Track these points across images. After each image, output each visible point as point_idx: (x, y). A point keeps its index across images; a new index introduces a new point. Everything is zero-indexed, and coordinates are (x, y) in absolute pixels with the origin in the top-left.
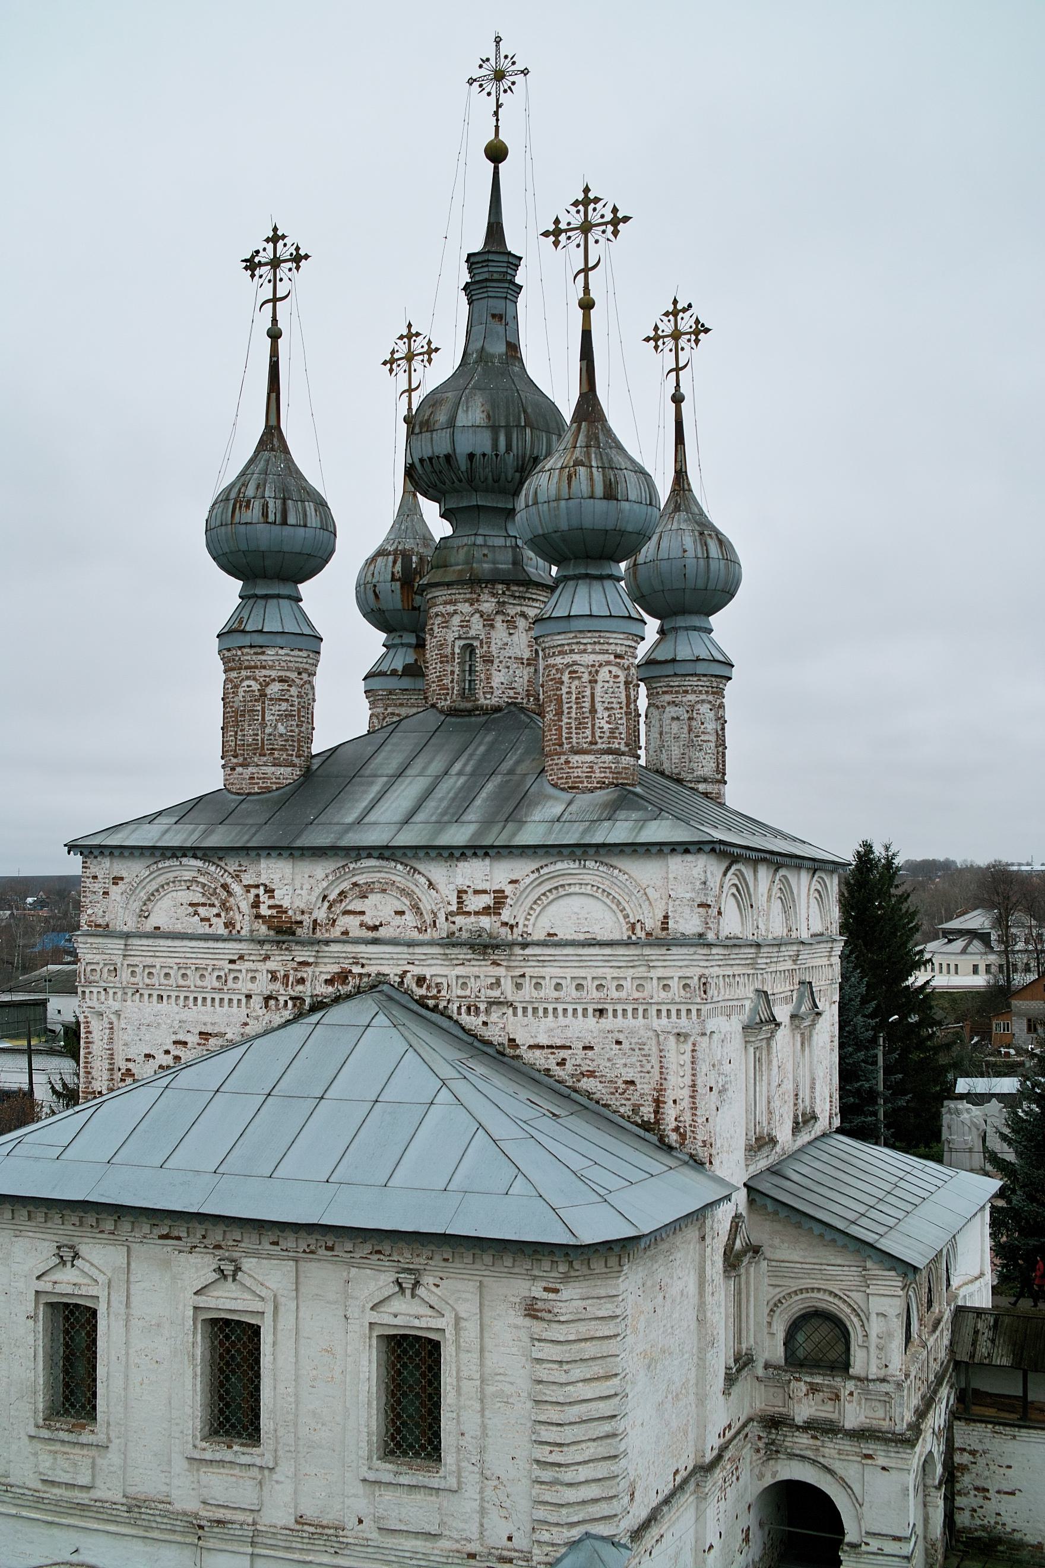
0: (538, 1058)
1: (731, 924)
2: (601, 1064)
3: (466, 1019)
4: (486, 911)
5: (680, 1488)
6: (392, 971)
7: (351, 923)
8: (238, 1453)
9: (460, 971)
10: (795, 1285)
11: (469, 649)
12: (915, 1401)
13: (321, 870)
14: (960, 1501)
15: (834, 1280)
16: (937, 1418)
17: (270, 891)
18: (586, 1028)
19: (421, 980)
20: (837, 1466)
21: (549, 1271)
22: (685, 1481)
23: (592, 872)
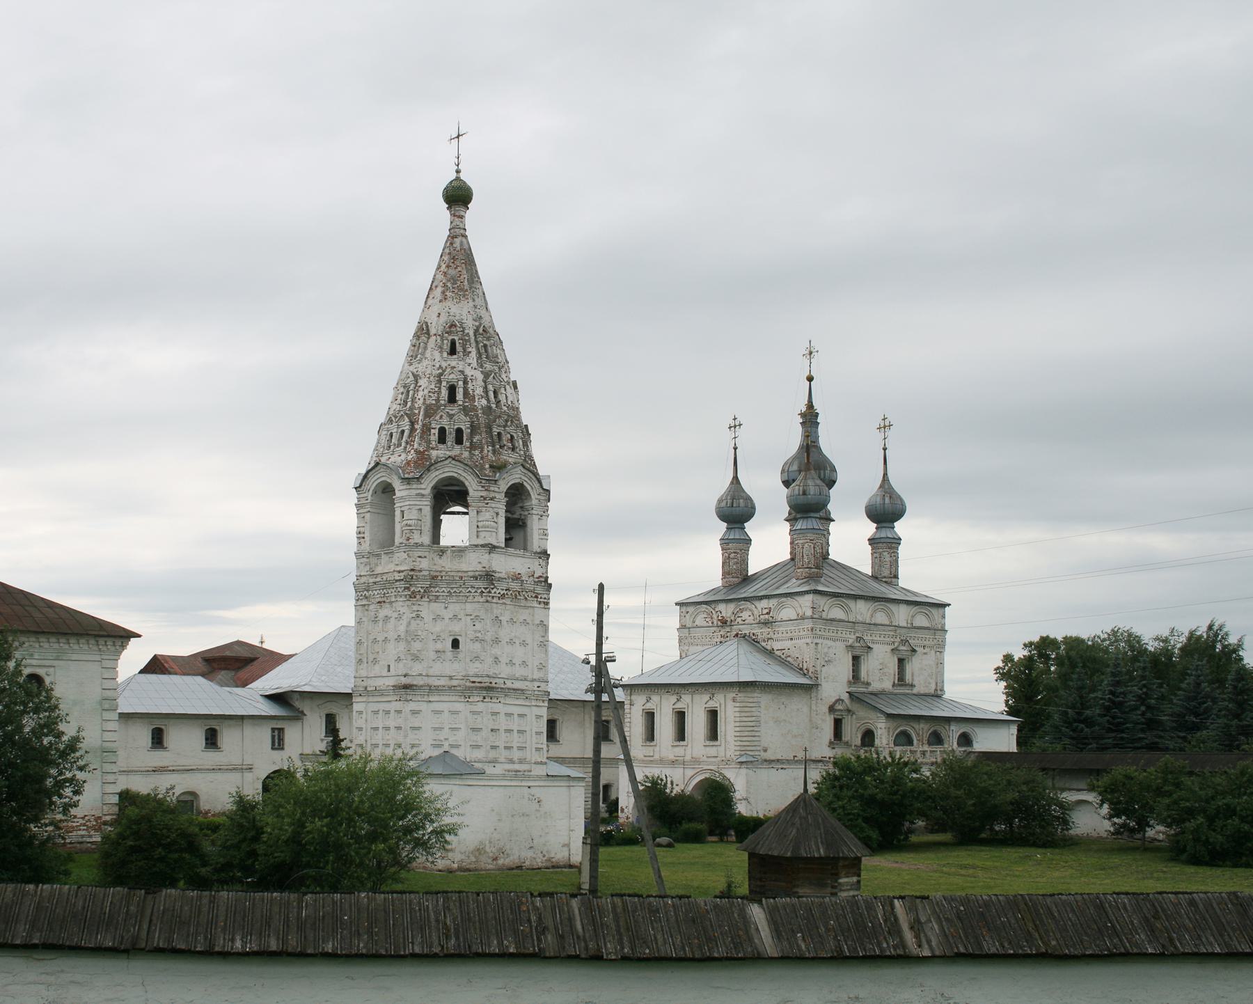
0: (778, 653)
8: (682, 743)
13: (732, 606)
18: (788, 644)
23: (789, 601)
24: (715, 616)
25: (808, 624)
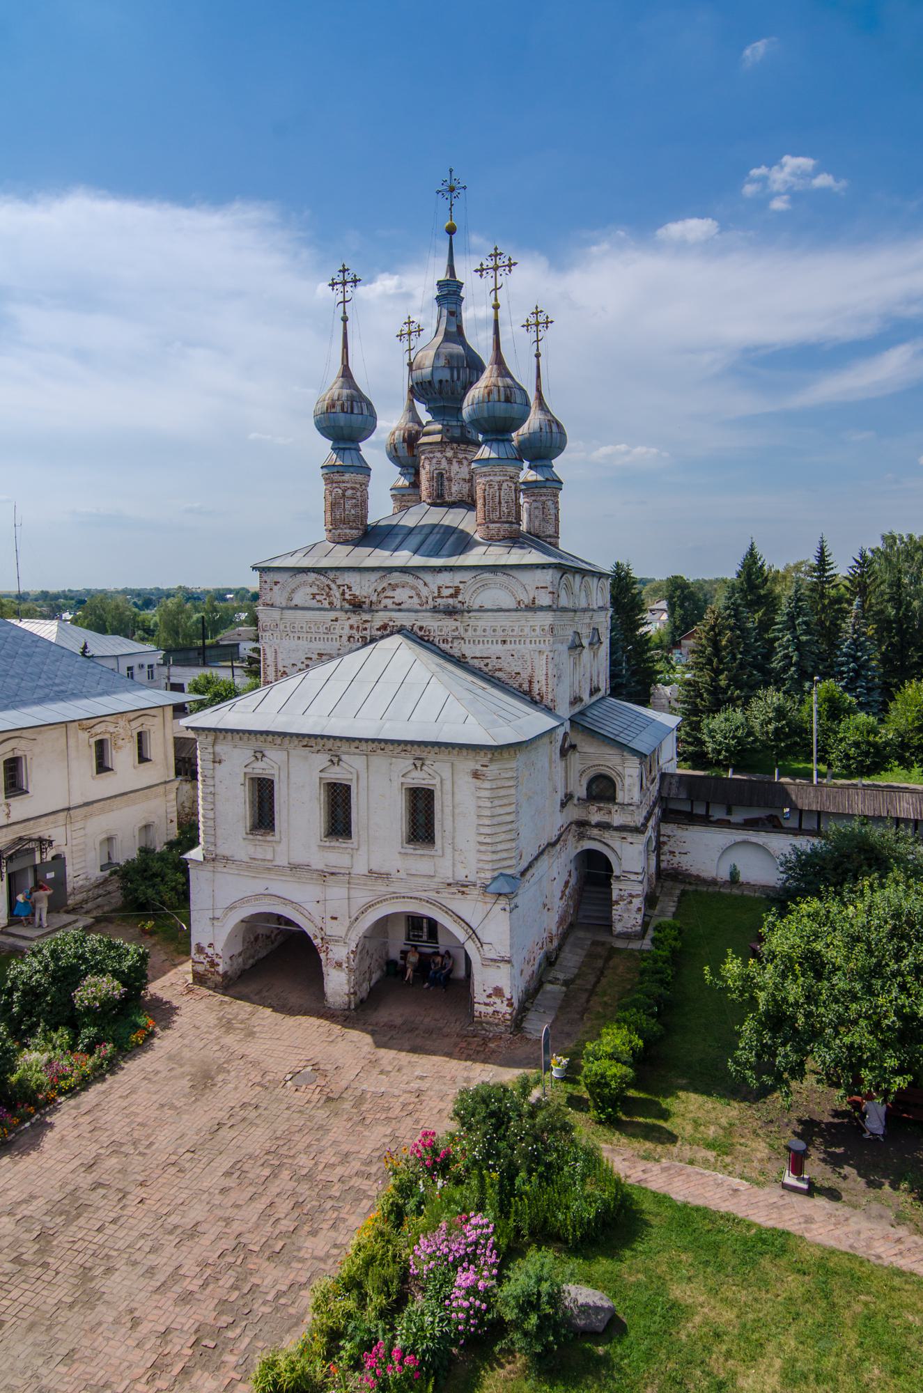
0: (476, 663)
1: (564, 601)
2: (504, 665)
3: (443, 646)
4: (451, 596)
5: (541, 853)
6: (408, 624)
7: (388, 602)
9: (440, 623)
10: (591, 763)
11: (441, 475)
12: (644, 813)
14: (662, 857)
15: (609, 760)
16: (652, 823)
17: (349, 588)
18: (498, 649)
19: (421, 628)
20: (610, 842)
21: (484, 758)
22: (544, 850)
24: (336, 593)
25: (546, 619)
